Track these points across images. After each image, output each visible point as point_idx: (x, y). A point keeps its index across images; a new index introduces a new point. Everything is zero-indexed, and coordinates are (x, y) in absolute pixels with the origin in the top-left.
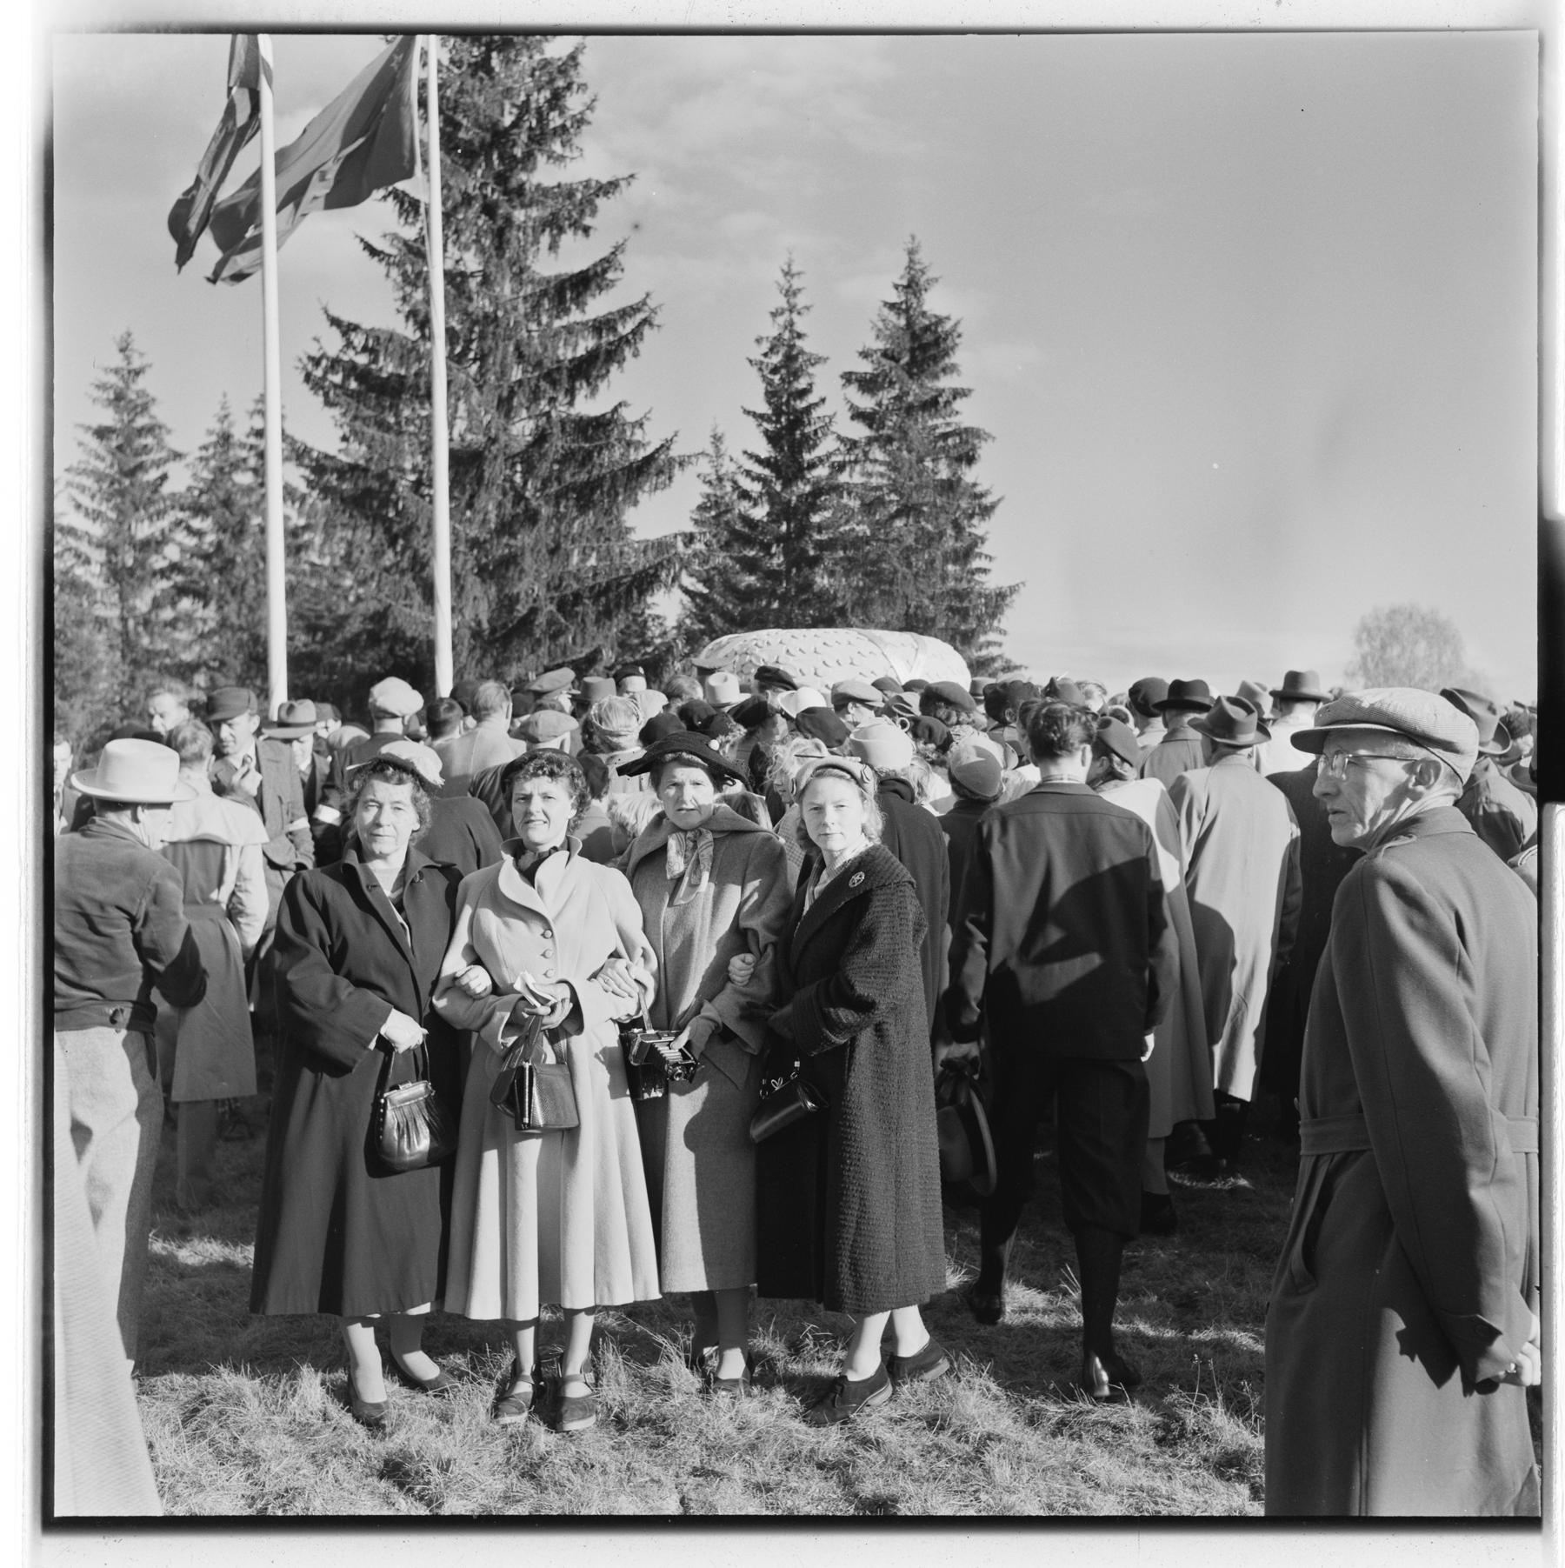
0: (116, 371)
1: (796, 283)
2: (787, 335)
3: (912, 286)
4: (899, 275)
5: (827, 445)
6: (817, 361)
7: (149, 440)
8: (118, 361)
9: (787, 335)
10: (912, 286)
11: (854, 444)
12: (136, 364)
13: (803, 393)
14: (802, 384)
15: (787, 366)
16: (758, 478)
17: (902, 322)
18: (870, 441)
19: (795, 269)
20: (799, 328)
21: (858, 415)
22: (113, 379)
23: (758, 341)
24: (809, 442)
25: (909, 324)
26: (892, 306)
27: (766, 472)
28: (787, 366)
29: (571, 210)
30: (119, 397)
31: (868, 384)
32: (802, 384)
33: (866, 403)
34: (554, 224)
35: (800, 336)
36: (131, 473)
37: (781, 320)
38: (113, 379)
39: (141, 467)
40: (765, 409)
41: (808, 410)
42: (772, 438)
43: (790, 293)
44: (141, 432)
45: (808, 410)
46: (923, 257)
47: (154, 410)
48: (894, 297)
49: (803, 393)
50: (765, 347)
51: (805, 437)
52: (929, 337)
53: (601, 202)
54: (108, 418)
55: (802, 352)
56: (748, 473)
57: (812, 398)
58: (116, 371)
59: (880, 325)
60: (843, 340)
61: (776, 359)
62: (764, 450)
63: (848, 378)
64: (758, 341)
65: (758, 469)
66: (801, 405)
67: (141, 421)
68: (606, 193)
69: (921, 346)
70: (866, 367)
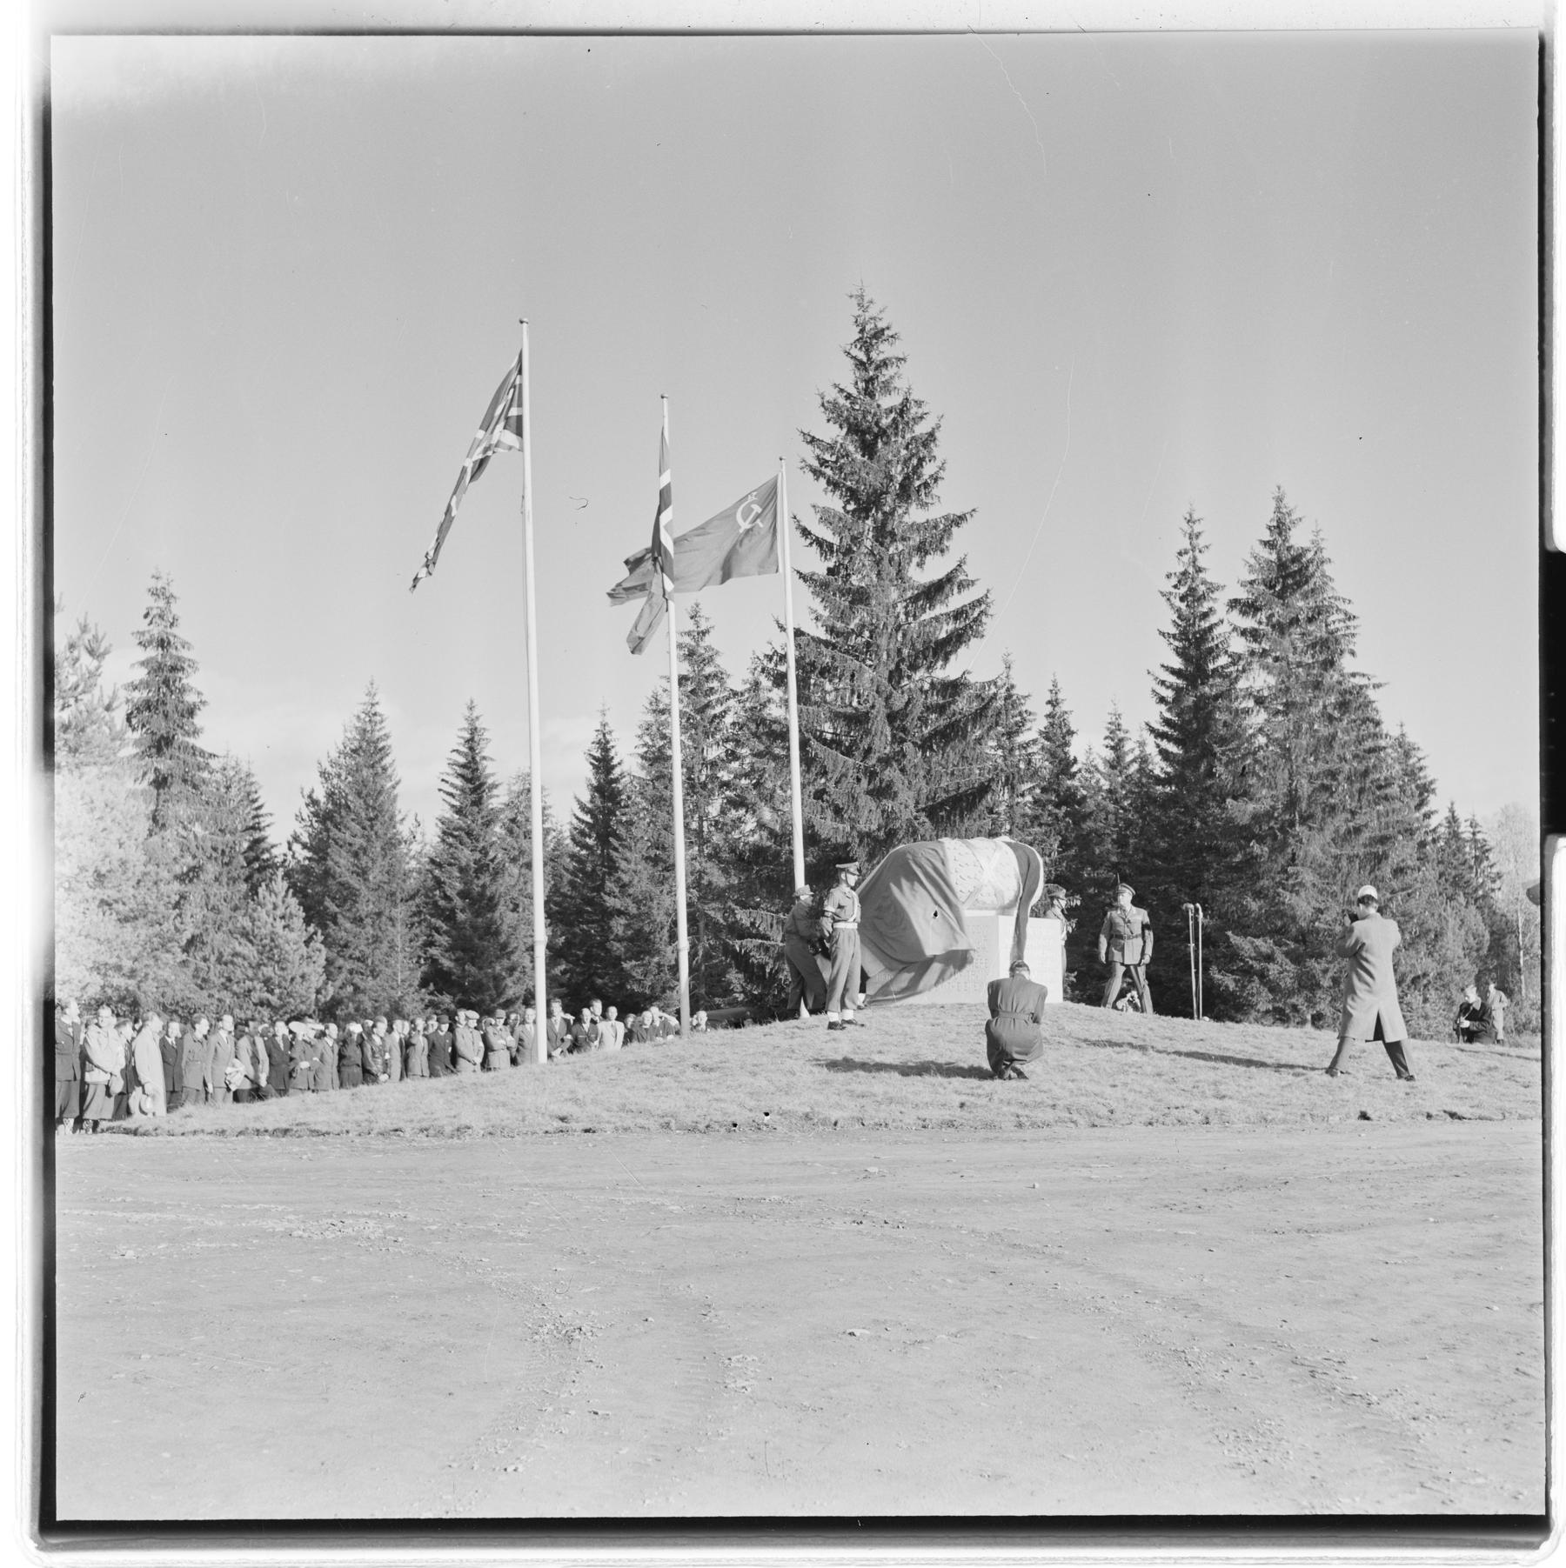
0: (689, 634)
1: (1197, 528)
2: (1191, 570)
3: (1280, 528)
4: (1269, 517)
5: (1223, 660)
6: (1212, 588)
7: (715, 684)
8: (690, 626)
9: (1191, 570)
10: (1280, 528)
11: (1240, 657)
12: (703, 628)
13: (1205, 616)
14: (1205, 607)
15: (1191, 592)
16: (1170, 687)
17: (1274, 557)
18: (1252, 653)
19: (1195, 517)
20: (1200, 563)
21: (1244, 633)
22: (687, 640)
23: (1169, 576)
24: (1212, 653)
25: (1279, 559)
26: (1266, 543)
27: (1180, 683)
28: (1191, 592)
29: (933, 539)
30: (691, 654)
31: (1249, 608)
32: (1205, 607)
33: (1248, 623)
34: (922, 550)
35: (1199, 570)
36: (701, 710)
37: (1185, 558)
38: (687, 640)
39: (707, 706)
40: (1174, 631)
41: (1211, 628)
42: (1181, 653)
43: (1193, 536)
44: (707, 678)
45: (1211, 628)
46: (1289, 502)
47: (718, 660)
48: (1267, 537)
49: (1205, 616)
50: (1174, 581)
51: (1211, 651)
52: (1295, 567)
53: (955, 529)
54: (685, 668)
55: (1204, 582)
56: (1163, 683)
57: (1213, 619)
58: (689, 634)
59: (1252, 561)
60: (1232, 570)
61: (1183, 590)
62: (1177, 663)
63: (1234, 603)
64: (1169, 576)
65: (1172, 679)
66: (1205, 624)
67: (708, 670)
68: (958, 525)
69: (1289, 574)
70: (1243, 595)
